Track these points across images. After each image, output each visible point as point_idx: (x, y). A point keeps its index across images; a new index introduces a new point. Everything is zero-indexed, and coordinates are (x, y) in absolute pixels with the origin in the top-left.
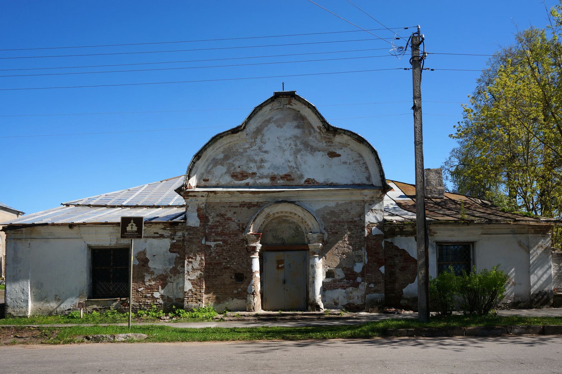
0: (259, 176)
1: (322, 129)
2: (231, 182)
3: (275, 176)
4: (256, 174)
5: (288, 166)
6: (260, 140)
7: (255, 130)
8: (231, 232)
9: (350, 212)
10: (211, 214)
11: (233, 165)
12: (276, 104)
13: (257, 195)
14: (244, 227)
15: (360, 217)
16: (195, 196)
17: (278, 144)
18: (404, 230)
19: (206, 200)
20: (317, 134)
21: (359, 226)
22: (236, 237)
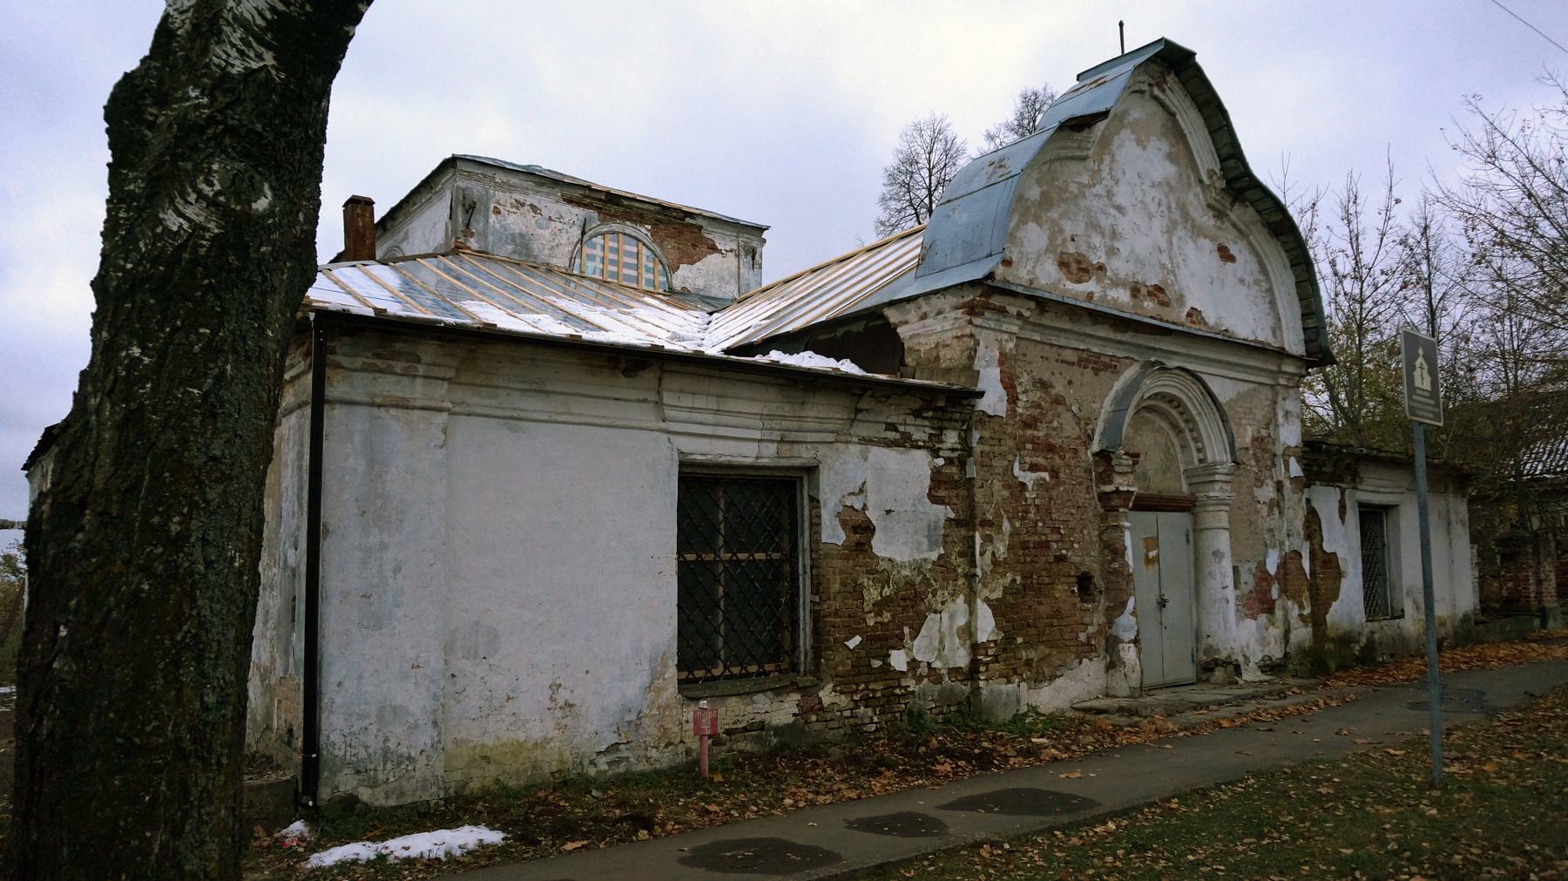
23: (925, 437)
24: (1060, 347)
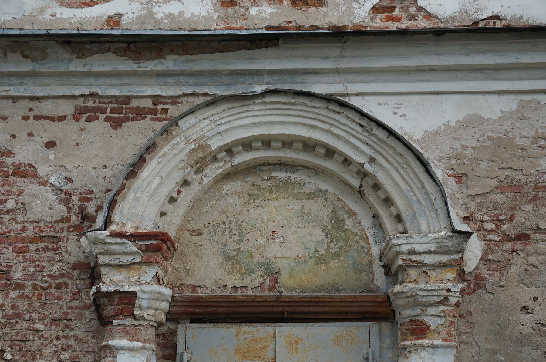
2: (42, 11)
8: (30, 233)
14: (91, 208)
22: (50, 254)
24: (32, 99)
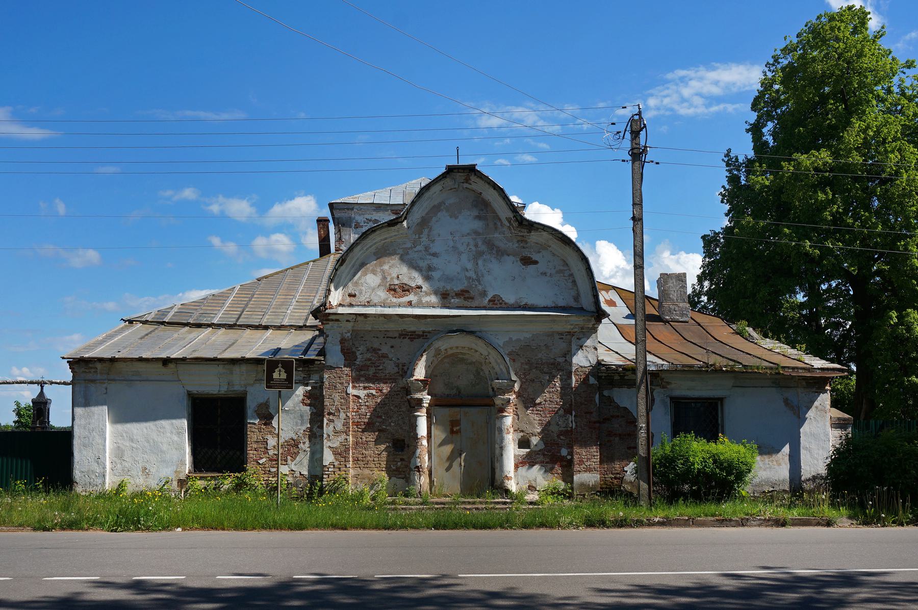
0: (425, 292)
1: (512, 222)
2: (387, 299)
3: (447, 292)
4: (422, 288)
5: (466, 276)
6: (426, 236)
7: (419, 221)
9: (551, 349)
10: (359, 349)
11: (390, 274)
12: (448, 182)
13: (423, 321)
14: (405, 368)
15: (565, 357)
16: (337, 320)
17: (452, 244)
18: (626, 377)
19: (353, 327)
20: (505, 229)
21: (563, 371)
23: (301, 378)
